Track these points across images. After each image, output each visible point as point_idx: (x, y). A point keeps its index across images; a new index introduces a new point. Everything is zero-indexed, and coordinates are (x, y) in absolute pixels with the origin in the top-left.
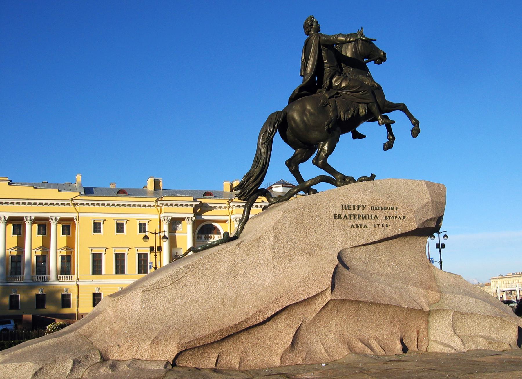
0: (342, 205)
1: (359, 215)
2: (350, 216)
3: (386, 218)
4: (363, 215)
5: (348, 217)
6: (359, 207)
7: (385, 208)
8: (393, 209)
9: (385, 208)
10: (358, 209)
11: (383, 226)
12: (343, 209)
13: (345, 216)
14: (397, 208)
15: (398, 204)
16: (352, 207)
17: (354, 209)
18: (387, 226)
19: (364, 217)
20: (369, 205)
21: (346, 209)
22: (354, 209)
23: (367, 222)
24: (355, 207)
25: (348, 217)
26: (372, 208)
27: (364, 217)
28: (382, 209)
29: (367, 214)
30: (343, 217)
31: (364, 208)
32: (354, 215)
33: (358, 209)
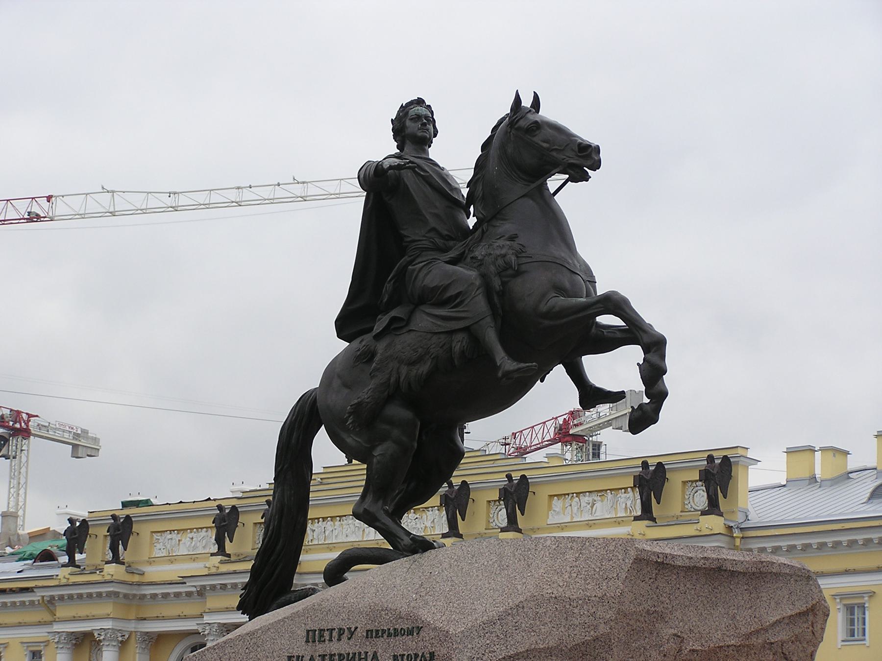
0: (308, 631)
4: (360, 653)
6: (341, 632)
7: (397, 633)
8: (410, 632)
9: (397, 633)
10: (339, 640)
12: (307, 641)
14: (419, 629)
15: (426, 615)
16: (327, 635)
17: (331, 640)
20: (362, 625)
21: (314, 641)
22: (331, 640)
24: (335, 634)
28: (389, 635)
29: (356, 649)
31: (352, 634)
33: (339, 640)
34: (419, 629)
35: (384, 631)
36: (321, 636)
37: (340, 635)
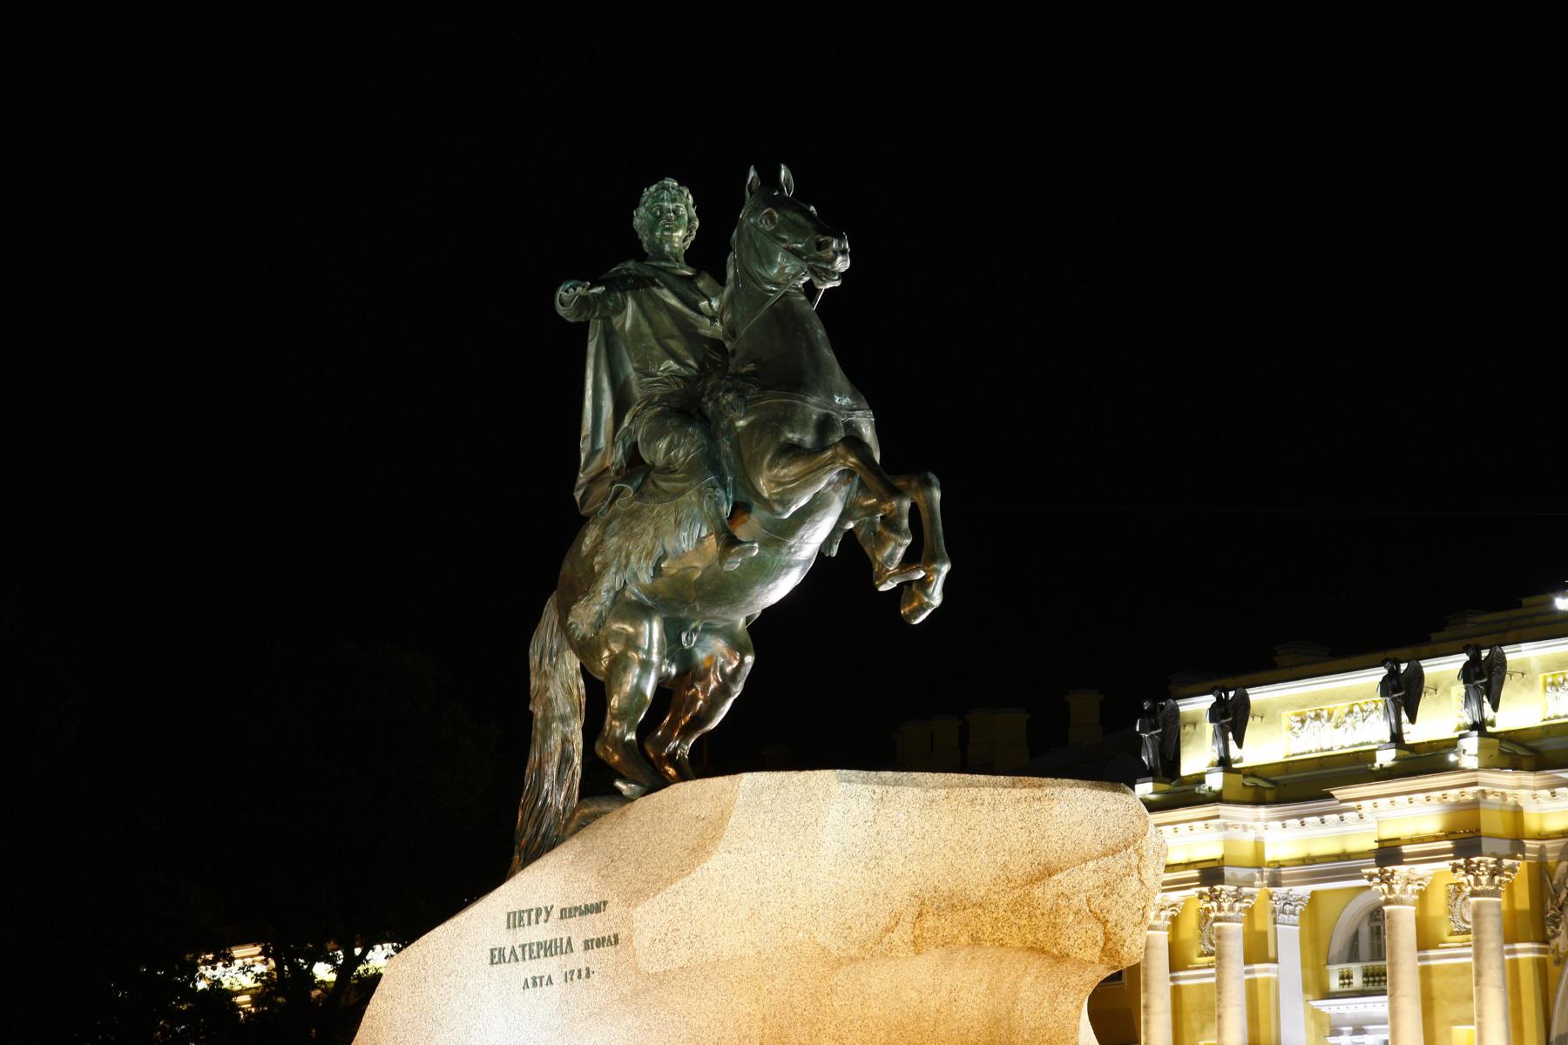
1: (539, 944)
2: (523, 947)
3: (588, 945)
5: (519, 952)
11: (579, 976)
13: (513, 951)
14: (605, 903)
16: (525, 916)
18: (588, 976)
19: (549, 949)
23: (550, 966)
24: (533, 917)
25: (519, 952)
26: (566, 914)
27: (549, 949)
30: (507, 953)
32: (531, 945)
34: (605, 903)
35: (576, 909)
36: (521, 919)
37: (538, 915)
